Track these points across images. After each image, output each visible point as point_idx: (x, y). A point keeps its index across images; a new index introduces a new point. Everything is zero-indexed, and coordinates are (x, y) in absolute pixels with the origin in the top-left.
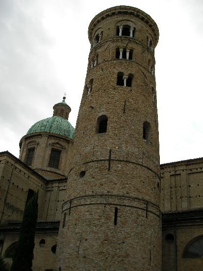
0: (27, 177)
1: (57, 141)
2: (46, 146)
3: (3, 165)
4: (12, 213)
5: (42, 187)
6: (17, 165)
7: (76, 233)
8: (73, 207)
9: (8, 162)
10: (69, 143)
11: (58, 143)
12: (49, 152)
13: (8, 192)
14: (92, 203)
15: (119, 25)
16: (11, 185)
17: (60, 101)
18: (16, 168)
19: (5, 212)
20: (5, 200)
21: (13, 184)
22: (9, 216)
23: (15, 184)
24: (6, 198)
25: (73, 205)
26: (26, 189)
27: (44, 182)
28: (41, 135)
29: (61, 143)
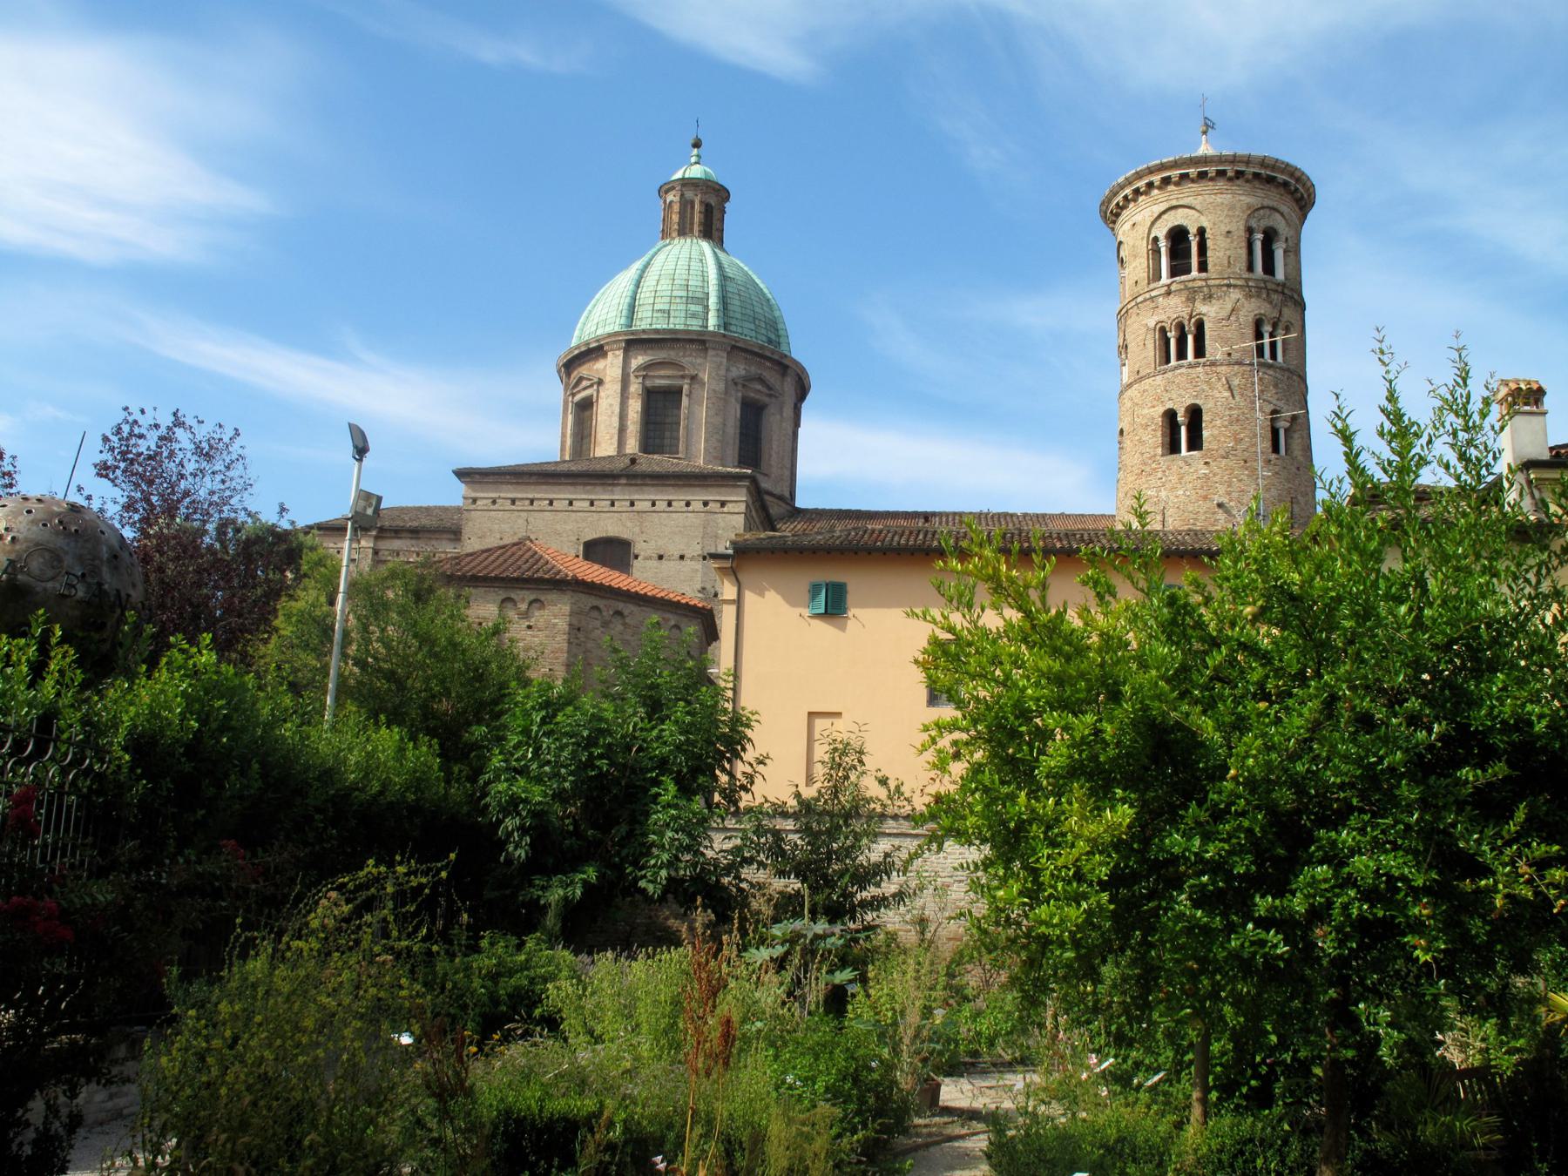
2: (726, 392)
12: (735, 410)
15: (1253, 224)
28: (703, 342)
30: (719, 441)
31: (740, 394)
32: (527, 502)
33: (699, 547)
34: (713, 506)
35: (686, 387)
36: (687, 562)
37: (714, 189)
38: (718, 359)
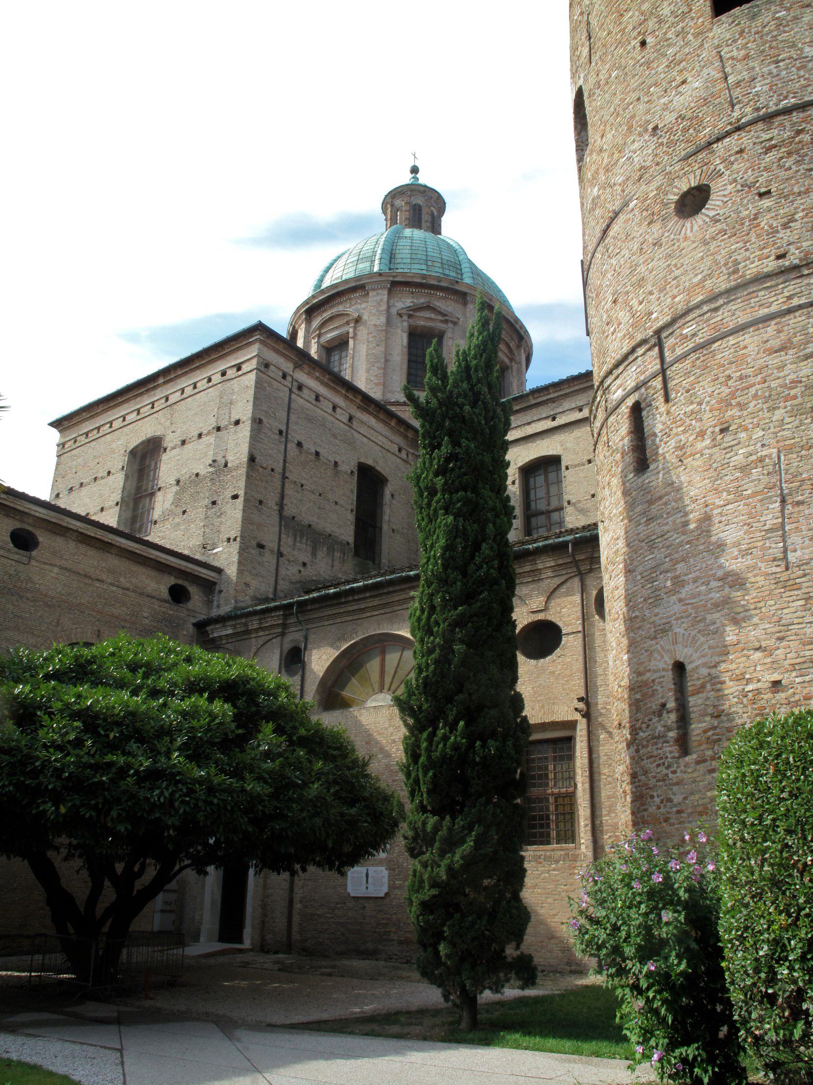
0: (345, 419)
1: (422, 300)
2: (389, 322)
3: (252, 376)
4: (314, 554)
5: (403, 455)
6: (302, 377)
7: (744, 469)
8: (678, 360)
9: (267, 366)
10: (465, 304)
11: (428, 307)
12: (401, 340)
13: (284, 477)
14: (795, 302)
16: (291, 446)
17: (406, 178)
18: (300, 387)
19: (284, 550)
20: (281, 506)
21: (299, 444)
22: (304, 564)
23: (308, 445)
24: (282, 497)
25: (679, 351)
26: (348, 465)
27: (406, 437)
28: (362, 287)
29: (441, 305)
30: (379, 368)
31: (406, 324)
32: (95, 432)
33: (214, 419)
34: (231, 373)
35: (351, 330)
36: (204, 439)
37: (419, 191)
38: (379, 298)
